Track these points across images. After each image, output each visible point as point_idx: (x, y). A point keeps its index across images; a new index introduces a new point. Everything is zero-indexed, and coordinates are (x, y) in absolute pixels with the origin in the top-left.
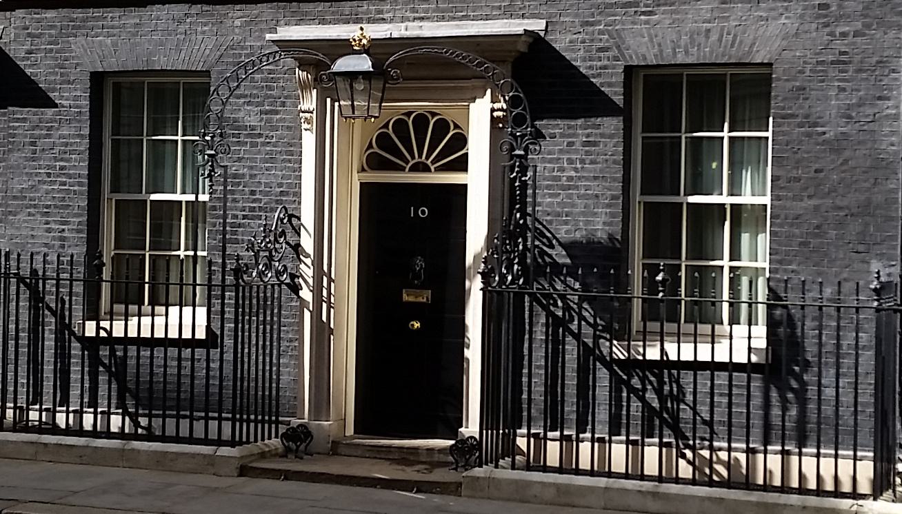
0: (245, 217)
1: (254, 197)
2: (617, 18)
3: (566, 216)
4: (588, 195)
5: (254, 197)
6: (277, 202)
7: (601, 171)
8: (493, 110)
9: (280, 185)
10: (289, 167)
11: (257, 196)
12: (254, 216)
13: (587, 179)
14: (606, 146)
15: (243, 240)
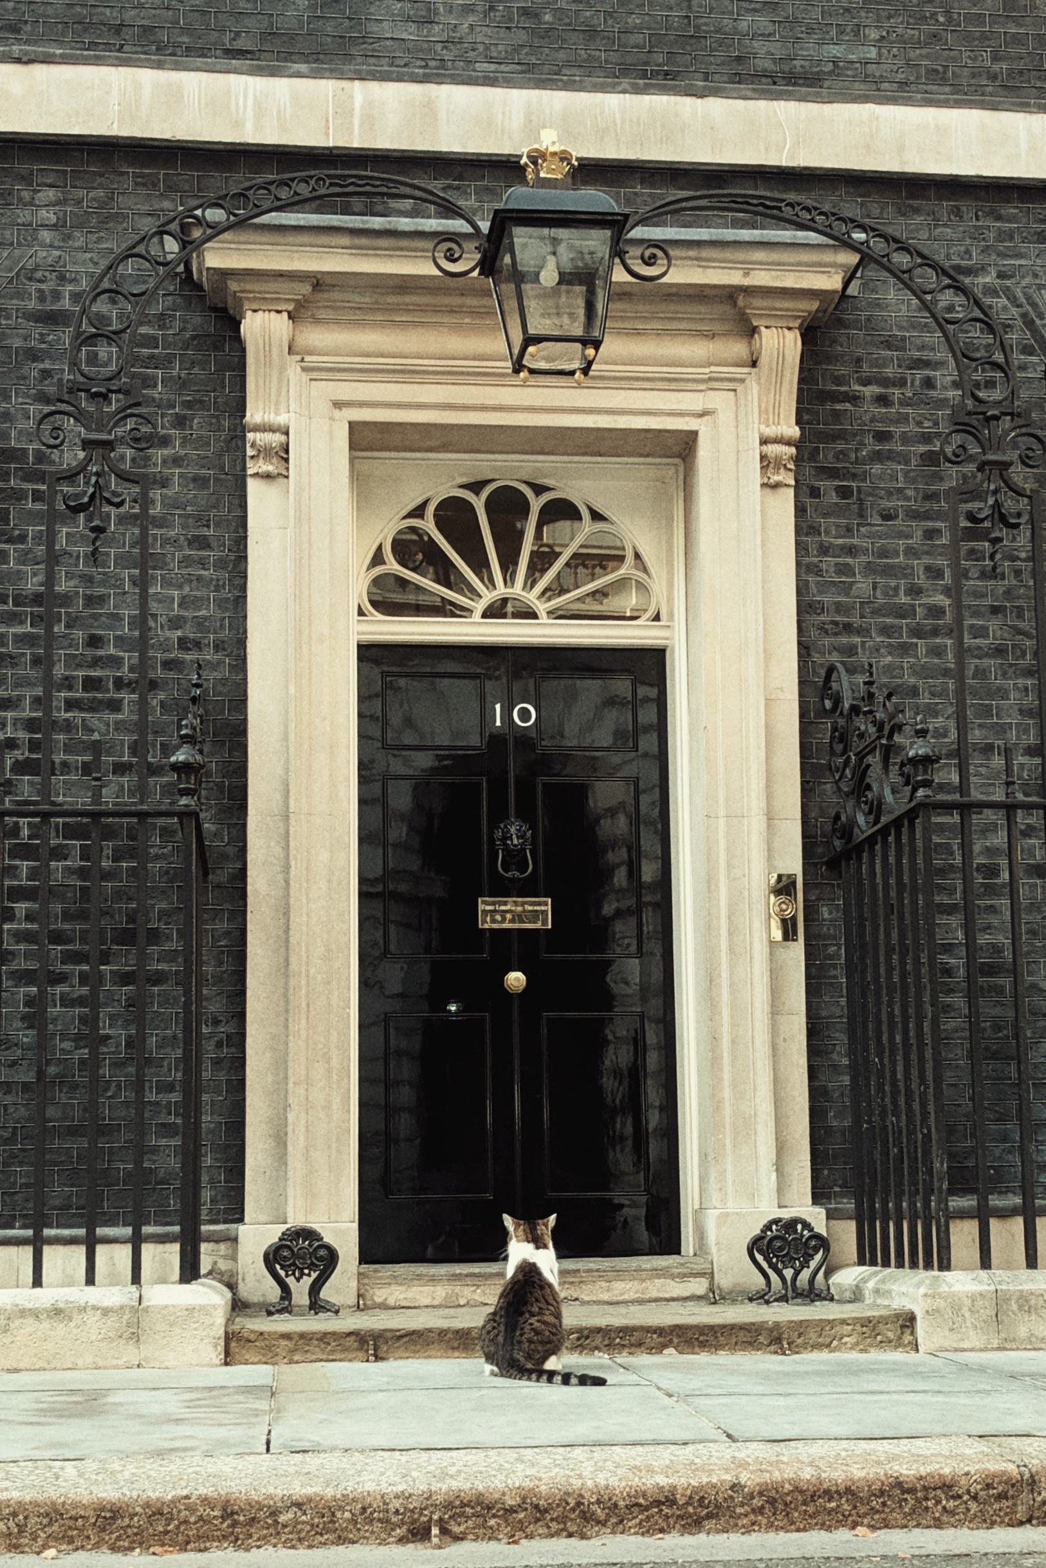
0: (70, 705)
1: (101, 653)
2: (1023, 262)
3: (933, 694)
4: (979, 648)
5: (101, 653)
6: (168, 665)
7: (1008, 592)
8: (764, 441)
9: (176, 623)
10: (199, 579)
11: (112, 651)
12: (101, 702)
13: (976, 614)
14: (1014, 540)
15: (65, 764)
